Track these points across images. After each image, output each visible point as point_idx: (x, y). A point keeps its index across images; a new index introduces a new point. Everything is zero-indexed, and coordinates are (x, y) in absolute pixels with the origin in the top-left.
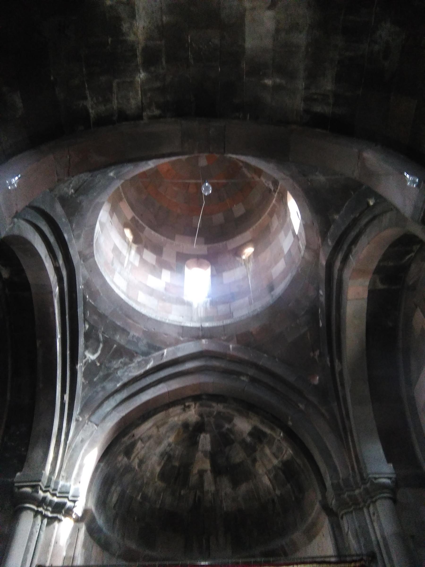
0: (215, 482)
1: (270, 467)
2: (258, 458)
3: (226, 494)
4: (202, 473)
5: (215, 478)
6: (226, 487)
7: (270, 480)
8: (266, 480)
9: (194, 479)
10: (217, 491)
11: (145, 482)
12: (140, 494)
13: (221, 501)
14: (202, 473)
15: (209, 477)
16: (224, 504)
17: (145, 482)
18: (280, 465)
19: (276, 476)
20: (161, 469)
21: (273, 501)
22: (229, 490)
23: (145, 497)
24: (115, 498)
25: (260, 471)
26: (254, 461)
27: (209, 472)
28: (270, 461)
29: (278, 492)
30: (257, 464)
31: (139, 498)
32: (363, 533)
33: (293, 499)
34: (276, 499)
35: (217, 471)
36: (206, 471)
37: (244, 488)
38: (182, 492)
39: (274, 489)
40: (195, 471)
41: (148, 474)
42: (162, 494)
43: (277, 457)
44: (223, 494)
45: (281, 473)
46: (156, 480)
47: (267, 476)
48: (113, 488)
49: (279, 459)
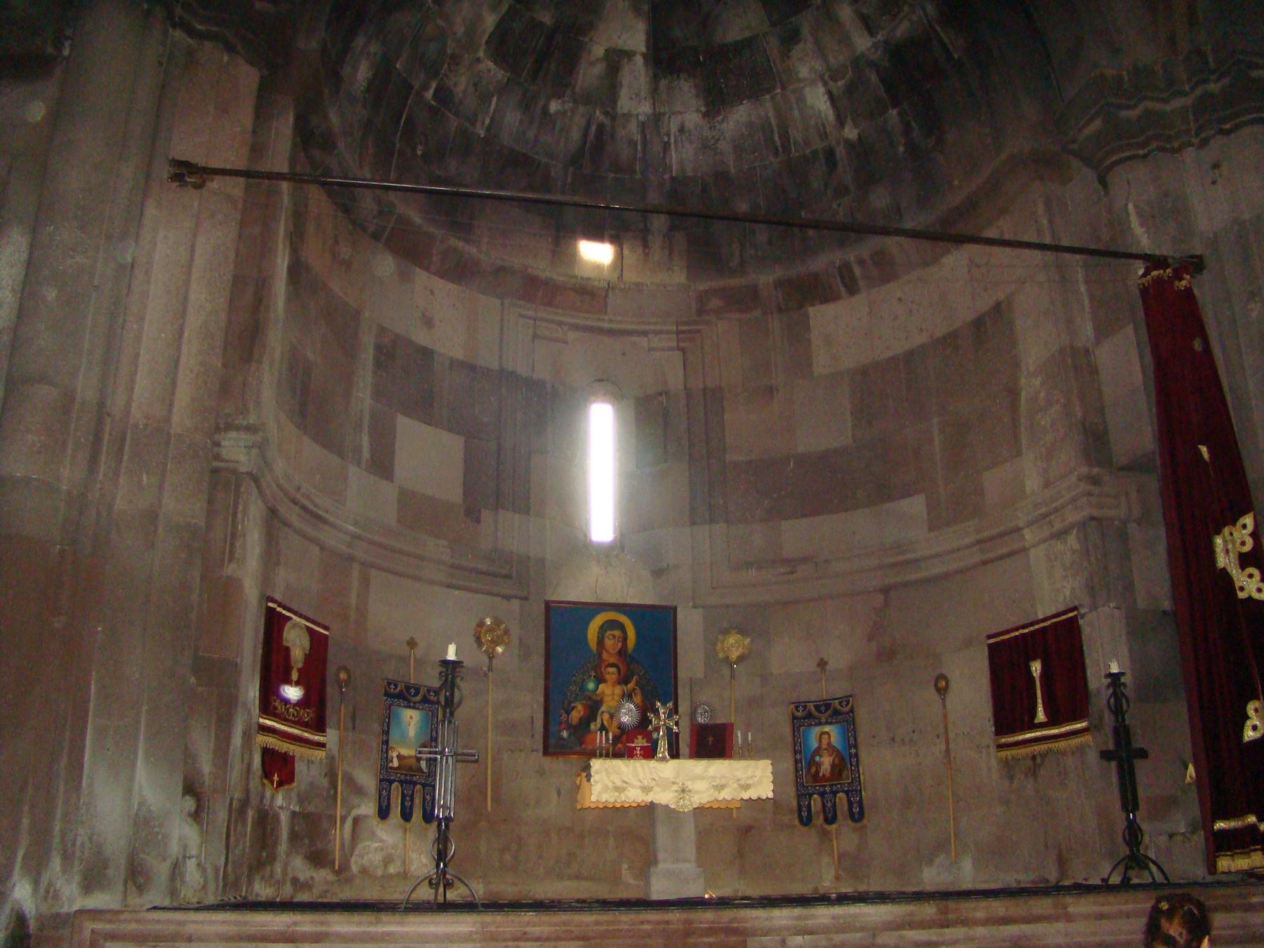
0: (654, 91)
1: (839, 58)
2: (805, 31)
3: (682, 129)
4: (616, 59)
5: (655, 78)
6: (687, 108)
7: (830, 95)
8: (818, 100)
9: (589, 73)
10: (657, 118)
11: (449, 51)
12: (434, 85)
13: (666, 146)
14: (616, 59)
15: (636, 76)
16: (674, 155)
17: (449, 51)
18: (876, 56)
19: (850, 89)
20: (498, 27)
21: (830, 154)
22: (693, 118)
23: (443, 95)
24: (362, 73)
25: (804, 72)
26: (792, 38)
27: (639, 60)
28: (845, 41)
29: (851, 133)
30: (797, 52)
31: (429, 95)
32: (1170, 210)
33: (901, 149)
34: (840, 151)
35: (665, 60)
36: (629, 55)
37: (739, 116)
38: (554, 106)
39: (841, 121)
40: (598, 51)
41: (460, 30)
42: (495, 99)
43: (871, 32)
44: (674, 129)
45: (874, 78)
46: (481, 54)
47: (825, 84)
48: (360, 41)
49: (880, 37)
